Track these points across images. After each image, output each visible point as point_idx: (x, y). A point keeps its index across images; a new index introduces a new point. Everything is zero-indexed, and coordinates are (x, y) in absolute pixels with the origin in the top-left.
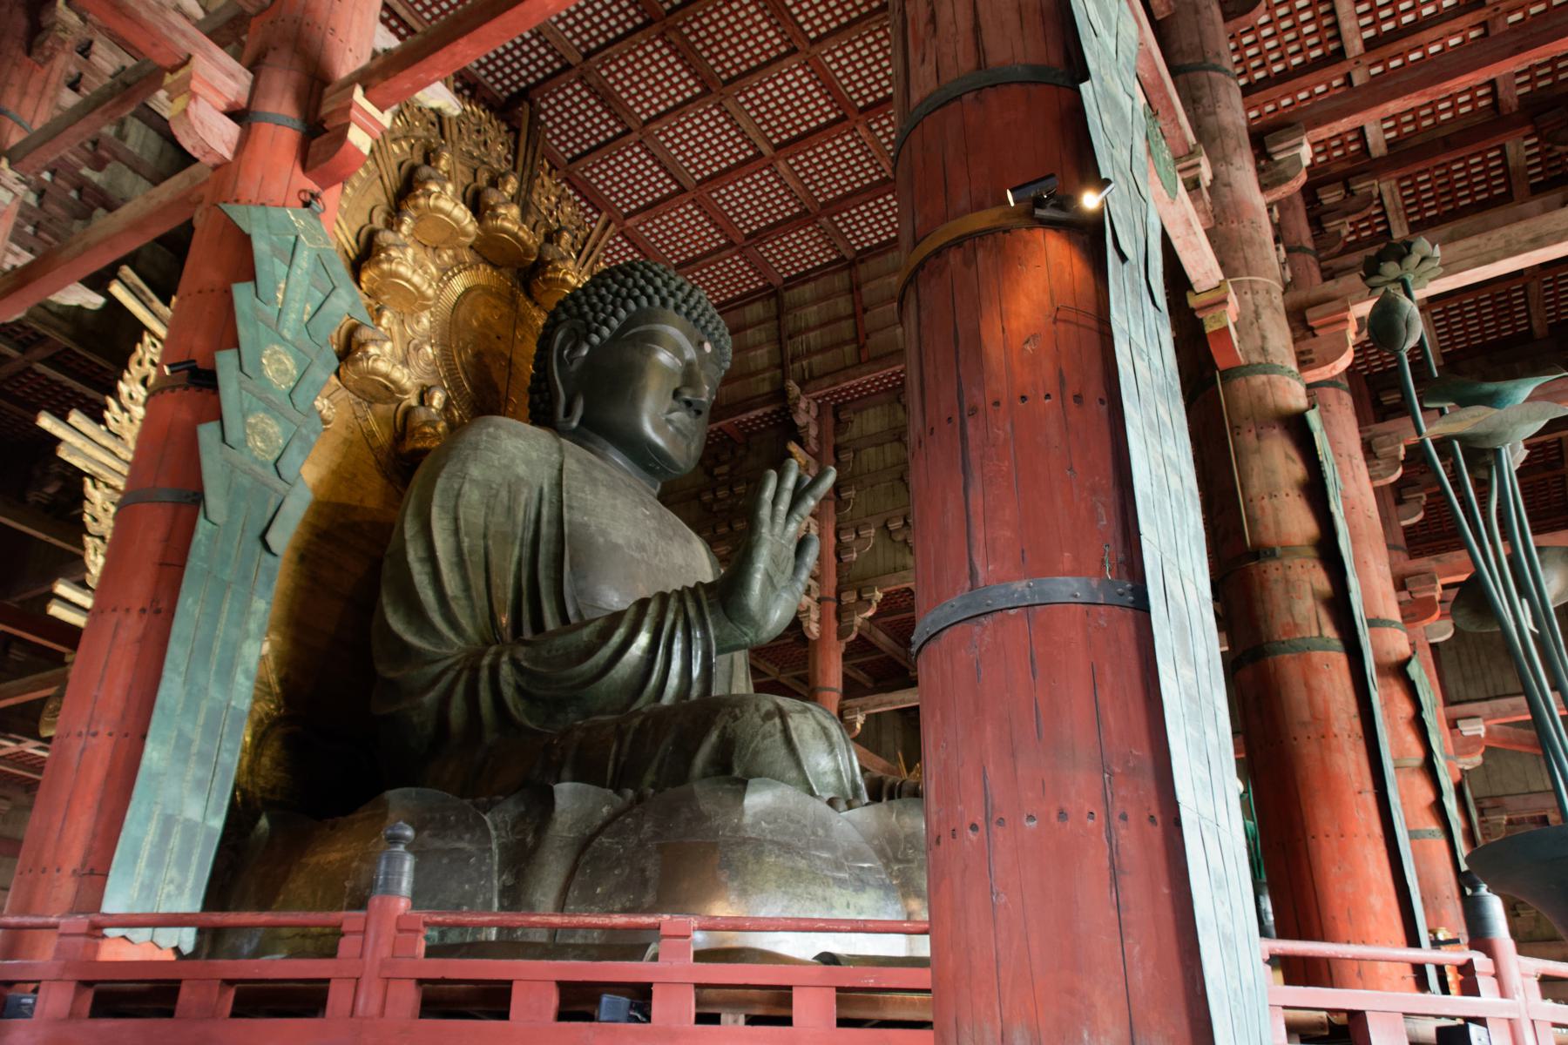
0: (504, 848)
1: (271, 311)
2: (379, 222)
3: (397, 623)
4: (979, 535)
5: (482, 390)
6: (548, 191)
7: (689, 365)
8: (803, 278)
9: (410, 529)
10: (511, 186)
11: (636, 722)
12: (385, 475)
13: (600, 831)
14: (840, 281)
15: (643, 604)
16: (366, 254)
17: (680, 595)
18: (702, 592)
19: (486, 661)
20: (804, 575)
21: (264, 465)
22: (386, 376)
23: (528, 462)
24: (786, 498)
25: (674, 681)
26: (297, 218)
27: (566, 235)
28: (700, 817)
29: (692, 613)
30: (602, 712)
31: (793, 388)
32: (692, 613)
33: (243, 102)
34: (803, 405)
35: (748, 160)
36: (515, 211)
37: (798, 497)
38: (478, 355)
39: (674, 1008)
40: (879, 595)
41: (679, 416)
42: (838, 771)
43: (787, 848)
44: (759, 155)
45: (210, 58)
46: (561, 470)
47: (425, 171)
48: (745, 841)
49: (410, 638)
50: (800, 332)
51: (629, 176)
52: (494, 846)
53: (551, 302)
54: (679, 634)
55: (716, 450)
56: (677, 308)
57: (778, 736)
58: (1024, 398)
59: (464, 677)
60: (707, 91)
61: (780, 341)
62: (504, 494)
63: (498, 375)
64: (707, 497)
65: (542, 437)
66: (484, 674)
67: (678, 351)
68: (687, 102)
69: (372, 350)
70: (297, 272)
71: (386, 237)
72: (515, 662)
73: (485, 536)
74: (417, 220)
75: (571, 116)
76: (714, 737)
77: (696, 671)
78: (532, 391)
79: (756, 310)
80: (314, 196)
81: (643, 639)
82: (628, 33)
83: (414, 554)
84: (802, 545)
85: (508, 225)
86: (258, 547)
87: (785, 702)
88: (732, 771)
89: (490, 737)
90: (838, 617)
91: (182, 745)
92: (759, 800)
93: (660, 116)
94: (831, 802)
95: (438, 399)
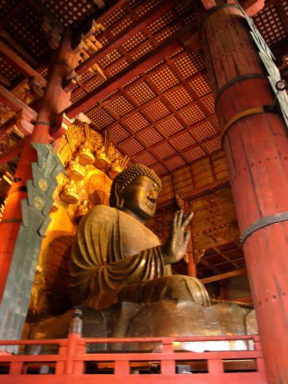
0: (108, 322)
1: (41, 170)
2: (70, 159)
3: (76, 262)
4: (261, 201)
5: (95, 199)
6: (112, 150)
8: (177, 169)
9: (79, 235)
10: (103, 148)
11: (143, 285)
12: (73, 223)
13: (136, 316)
14: (187, 169)
15: (143, 252)
16: (68, 166)
17: (153, 249)
18: (159, 248)
19: (100, 270)
20: (187, 242)
21: (39, 211)
22: (72, 197)
23: (110, 216)
24: (180, 221)
25: (153, 273)
26: (48, 146)
27: (117, 161)
28: (165, 311)
29: (157, 254)
30: (133, 283)
31: (177, 197)
32: (157, 254)
33: (35, 119)
34: (180, 201)
35: (162, 140)
36: (104, 155)
38: (96, 191)
39: (168, 369)
40: (204, 250)
41: (150, 203)
42: (202, 296)
43: (191, 319)
44: (165, 138)
45: (27, 109)
46: (118, 218)
47: (82, 146)
48: (179, 317)
49: (81, 266)
50: (178, 183)
51: (132, 145)
52: (105, 322)
53: (114, 177)
54: (153, 260)
55: (159, 211)
56: (147, 176)
57: (184, 287)
58: (268, 159)
59: (95, 274)
60: (151, 124)
61: (173, 186)
62: (104, 225)
63: (100, 196)
64: (156, 227)
65: (114, 210)
66: (100, 274)
68: (146, 127)
69: (69, 190)
70: (48, 160)
71: (72, 162)
72: (108, 270)
73: (99, 236)
74: (80, 158)
75: (117, 131)
76: (166, 288)
77: (159, 270)
78: (110, 199)
79: (166, 178)
80: (53, 141)
81: (143, 262)
82: (131, 111)
83: (80, 243)
84: (185, 234)
86: (37, 234)
87: (185, 277)
88: (172, 296)
89: (102, 292)
90: (194, 258)
91: (14, 292)
92: (182, 304)
93: (139, 131)
94: (202, 305)
95: (86, 202)
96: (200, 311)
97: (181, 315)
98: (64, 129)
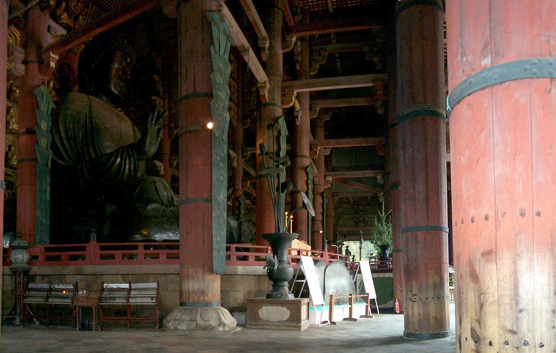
7: (123, 67)
15: (117, 150)
24: (155, 119)
25: (127, 171)
27: (81, 17)
37: (158, 118)
42: (168, 195)
43: (157, 217)
48: (148, 216)
54: (127, 158)
65: (83, 96)
67: (120, 64)
77: (132, 169)
81: (119, 160)
85: (65, 22)
90: (169, 131)
92: (151, 206)
96: (164, 211)
97: (149, 214)
98: (52, 68)
